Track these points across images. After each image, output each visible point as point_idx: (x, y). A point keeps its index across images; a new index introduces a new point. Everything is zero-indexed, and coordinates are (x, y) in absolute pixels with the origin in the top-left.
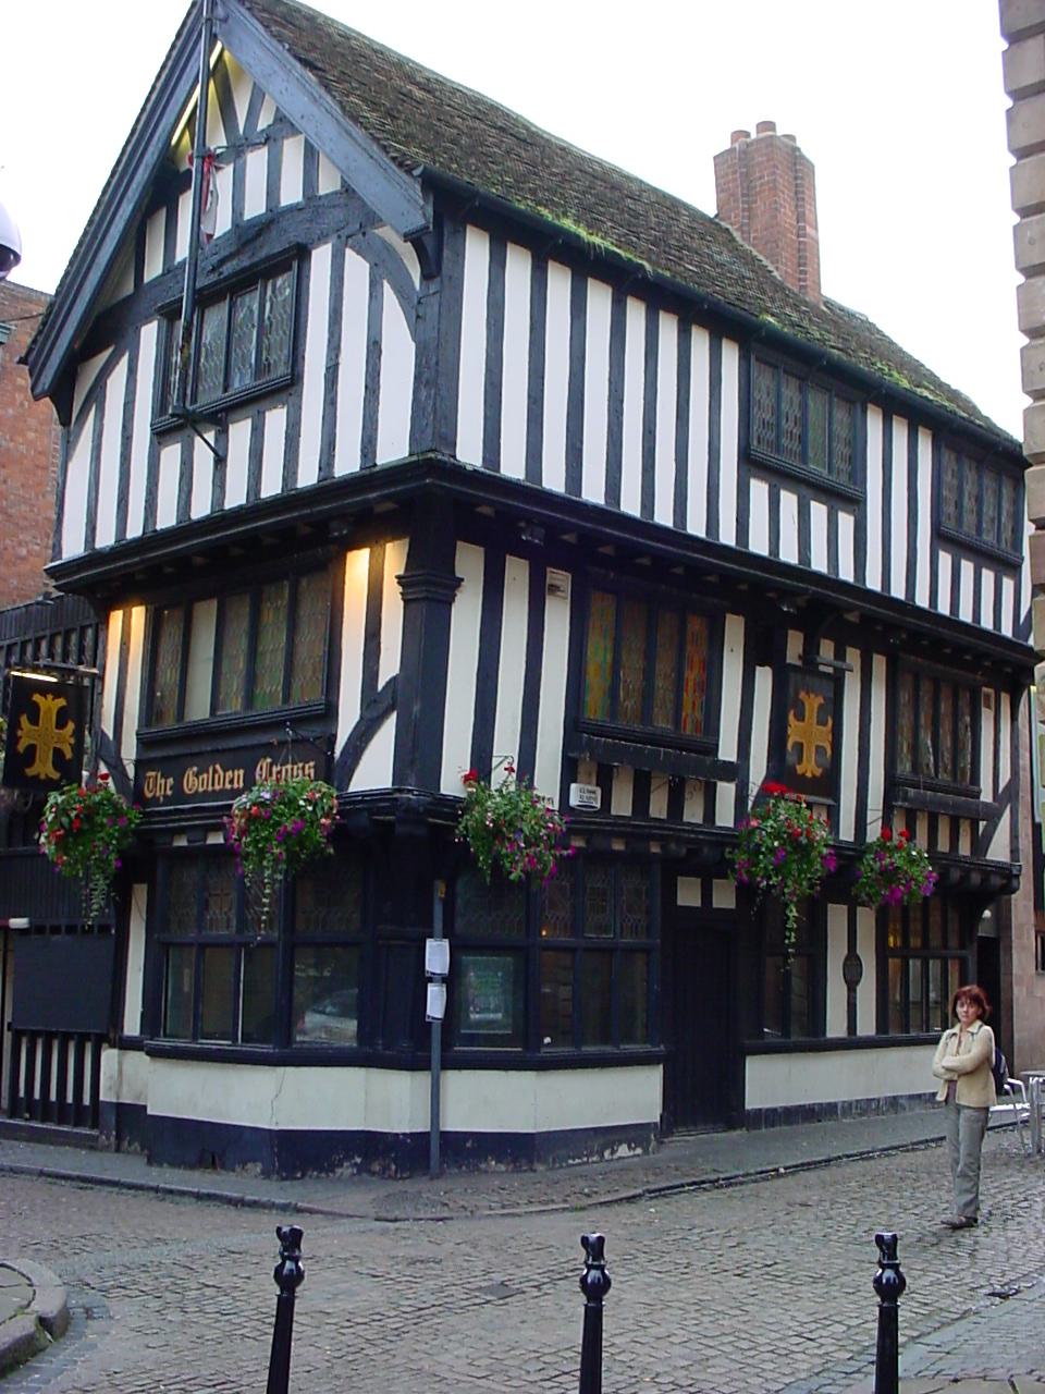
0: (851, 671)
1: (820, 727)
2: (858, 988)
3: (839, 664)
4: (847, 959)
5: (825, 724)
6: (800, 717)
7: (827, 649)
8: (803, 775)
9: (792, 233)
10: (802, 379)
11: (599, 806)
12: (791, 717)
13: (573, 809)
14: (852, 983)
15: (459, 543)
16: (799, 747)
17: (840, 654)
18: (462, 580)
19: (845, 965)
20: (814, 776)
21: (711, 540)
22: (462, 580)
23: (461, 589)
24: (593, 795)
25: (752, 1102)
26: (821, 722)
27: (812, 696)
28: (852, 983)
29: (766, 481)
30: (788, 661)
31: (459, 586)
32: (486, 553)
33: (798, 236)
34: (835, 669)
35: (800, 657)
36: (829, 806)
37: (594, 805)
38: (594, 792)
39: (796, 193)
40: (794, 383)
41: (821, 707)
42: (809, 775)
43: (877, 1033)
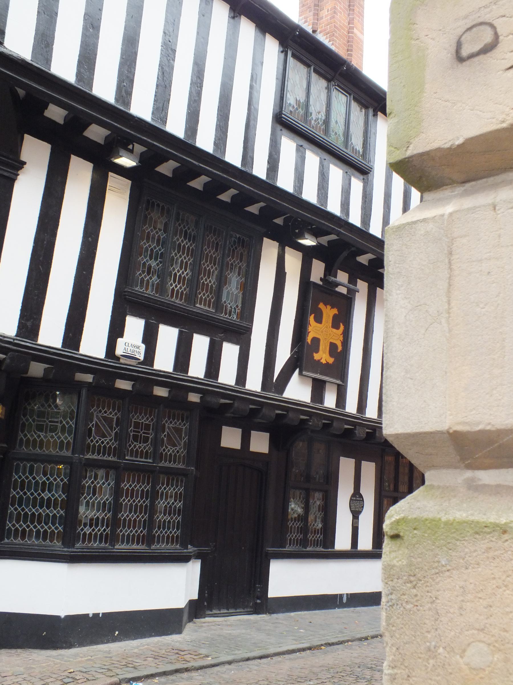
0: (358, 292)
1: (334, 330)
2: (361, 517)
3: (351, 286)
4: (353, 495)
5: (338, 328)
6: (319, 320)
7: (342, 277)
8: (319, 361)
9: (344, 30)
10: (329, 80)
11: (142, 358)
12: (311, 319)
13: (118, 359)
14: (356, 514)
15: (27, 137)
16: (316, 341)
17: (352, 280)
18: (25, 163)
19: (351, 499)
20: (327, 363)
21: (243, 169)
22: (25, 163)
23: (23, 169)
24: (138, 350)
25: (272, 593)
26: (335, 325)
27: (329, 307)
28: (356, 514)
29: (295, 141)
30: (312, 279)
31: (21, 168)
32: (52, 149)
33: (349, 33)
34: (349, 290)
35: (321, 279)
36: (339, 385)
37: (137, 356)
38: (138, 347)
39: (349, 6)
40: (323, 83)
41: (335, 317)
42: (323, 361)
43: (373, 548)
